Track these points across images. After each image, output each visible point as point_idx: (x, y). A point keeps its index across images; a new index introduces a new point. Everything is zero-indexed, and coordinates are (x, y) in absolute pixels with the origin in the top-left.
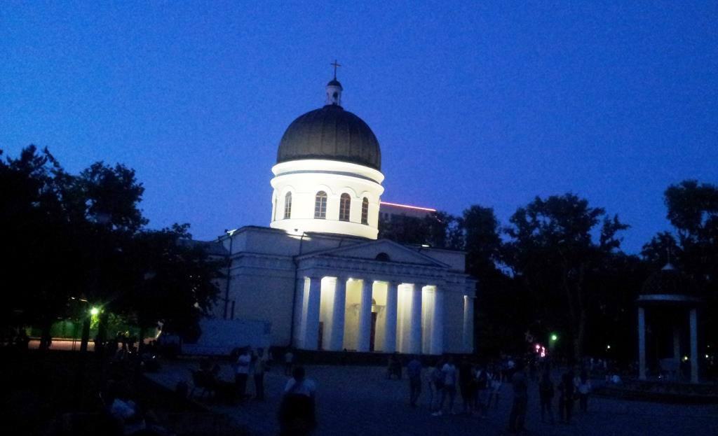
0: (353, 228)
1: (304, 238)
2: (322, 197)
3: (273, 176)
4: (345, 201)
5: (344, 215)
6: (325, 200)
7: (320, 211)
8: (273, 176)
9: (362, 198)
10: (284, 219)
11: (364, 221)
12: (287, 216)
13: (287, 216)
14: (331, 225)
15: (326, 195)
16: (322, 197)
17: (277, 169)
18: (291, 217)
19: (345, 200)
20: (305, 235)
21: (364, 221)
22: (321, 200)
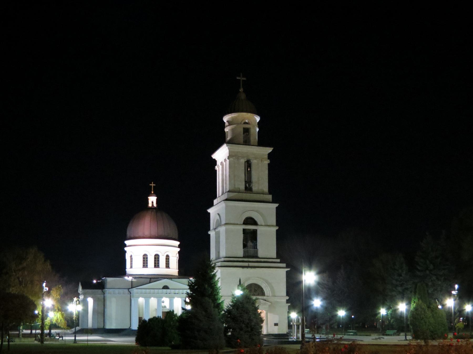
0: (162, 270)
1: (133, 280)
2: (145, 257)
3: (125, 246)
4: (157, 258)
5: (157, 265)
6: (147, 258)
7: (145, 264)
8: (125, 246)
9: (165, 255)
10: (130, 268)
11: (168, 266)
12: (131, 267)
13: (131, 267)
14: (151, 270)
15: (147, 256)
16: (145, 257)
17: (127, 242)
18: (133, 267)
19: (157, 257)
20: (133, 279)
21: (168, 266)
22: (145, 258)
